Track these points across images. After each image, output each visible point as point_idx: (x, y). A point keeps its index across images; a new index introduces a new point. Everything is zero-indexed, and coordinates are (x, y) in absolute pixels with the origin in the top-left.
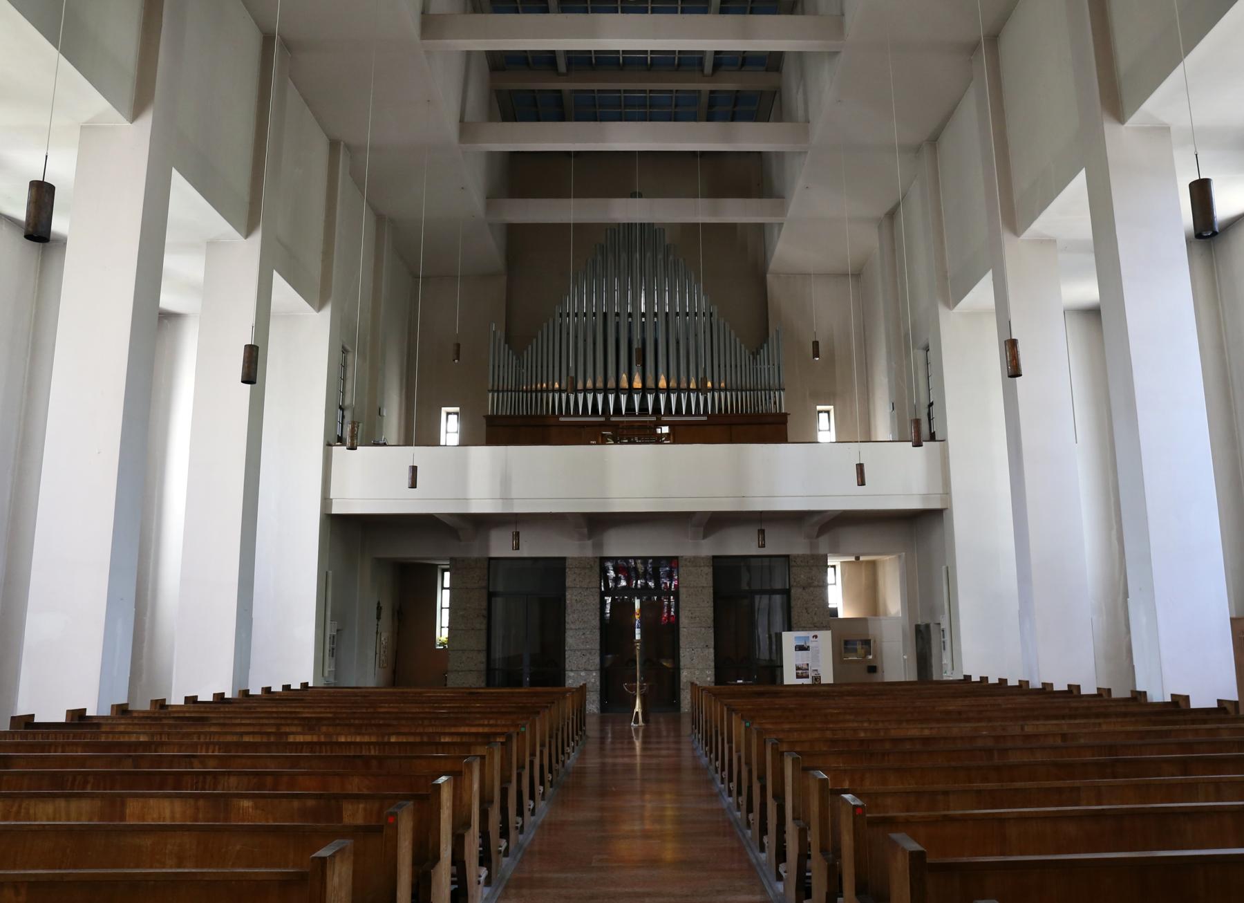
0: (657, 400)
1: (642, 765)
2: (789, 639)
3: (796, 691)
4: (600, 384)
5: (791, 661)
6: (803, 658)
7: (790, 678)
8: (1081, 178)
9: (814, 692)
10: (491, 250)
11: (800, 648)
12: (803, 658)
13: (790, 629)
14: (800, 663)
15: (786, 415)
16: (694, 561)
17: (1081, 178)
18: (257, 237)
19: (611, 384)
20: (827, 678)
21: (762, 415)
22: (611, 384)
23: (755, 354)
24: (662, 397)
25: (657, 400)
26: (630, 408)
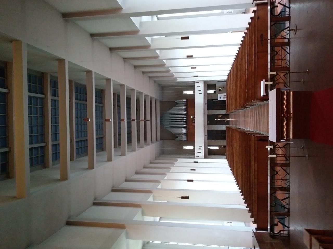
0: (184, 118)
1: (235, 119)
2: (219, 99)
3: (227, 98)
4: (182, 125)
5: (222, 99)
6: (222, 98)
7: (225, 99)
8: (164, 60)
9: (227, 96)
10: (162, 141)
11: (220, 98)
12: (222, 98)
13: (218, 99)
14: (223, 98)
15: (187, 99)
16: (208, 112)
17: (164, 60)
18: (171, 167)
19: (182, 124)
20: (225, 94)
21: (187, 103)
22: (182, 124)
23: (177, 104)
24: (184, 117)
25: (184, 118)
26: (185, 121)
